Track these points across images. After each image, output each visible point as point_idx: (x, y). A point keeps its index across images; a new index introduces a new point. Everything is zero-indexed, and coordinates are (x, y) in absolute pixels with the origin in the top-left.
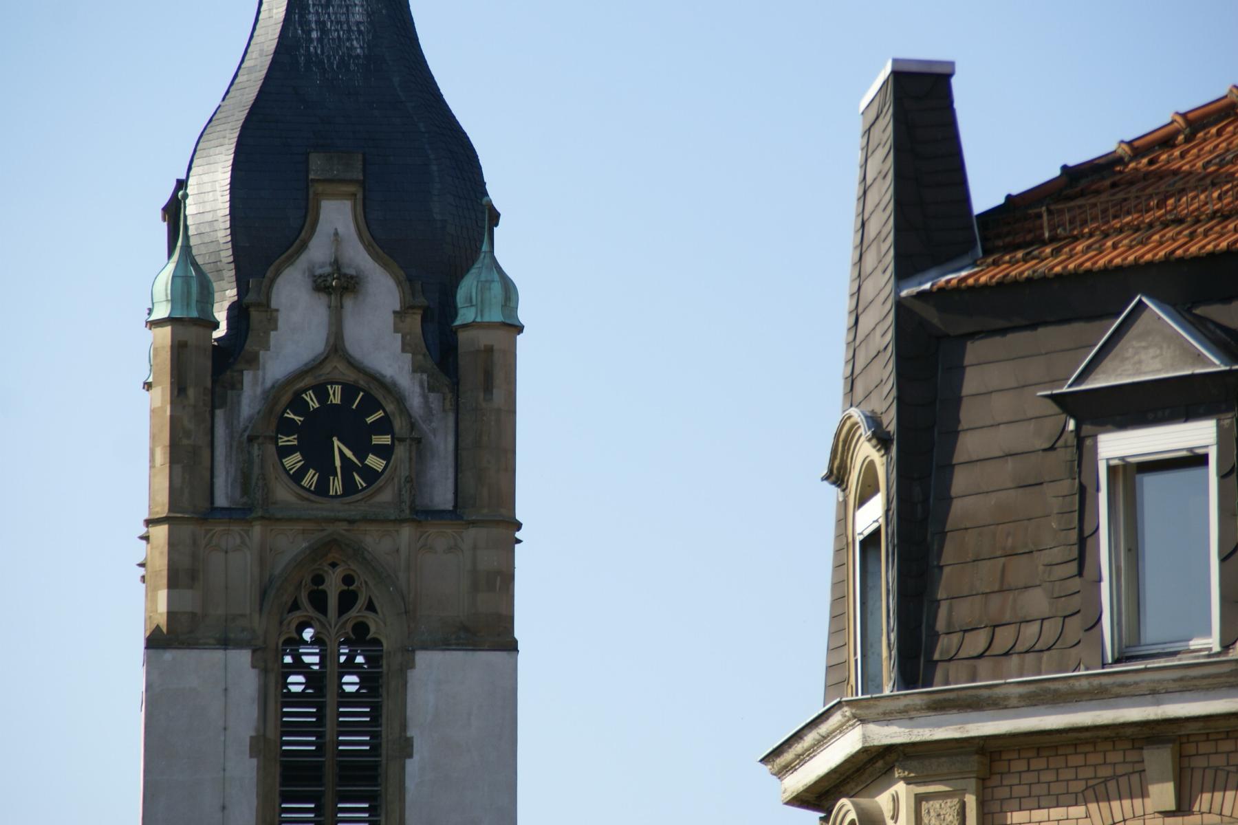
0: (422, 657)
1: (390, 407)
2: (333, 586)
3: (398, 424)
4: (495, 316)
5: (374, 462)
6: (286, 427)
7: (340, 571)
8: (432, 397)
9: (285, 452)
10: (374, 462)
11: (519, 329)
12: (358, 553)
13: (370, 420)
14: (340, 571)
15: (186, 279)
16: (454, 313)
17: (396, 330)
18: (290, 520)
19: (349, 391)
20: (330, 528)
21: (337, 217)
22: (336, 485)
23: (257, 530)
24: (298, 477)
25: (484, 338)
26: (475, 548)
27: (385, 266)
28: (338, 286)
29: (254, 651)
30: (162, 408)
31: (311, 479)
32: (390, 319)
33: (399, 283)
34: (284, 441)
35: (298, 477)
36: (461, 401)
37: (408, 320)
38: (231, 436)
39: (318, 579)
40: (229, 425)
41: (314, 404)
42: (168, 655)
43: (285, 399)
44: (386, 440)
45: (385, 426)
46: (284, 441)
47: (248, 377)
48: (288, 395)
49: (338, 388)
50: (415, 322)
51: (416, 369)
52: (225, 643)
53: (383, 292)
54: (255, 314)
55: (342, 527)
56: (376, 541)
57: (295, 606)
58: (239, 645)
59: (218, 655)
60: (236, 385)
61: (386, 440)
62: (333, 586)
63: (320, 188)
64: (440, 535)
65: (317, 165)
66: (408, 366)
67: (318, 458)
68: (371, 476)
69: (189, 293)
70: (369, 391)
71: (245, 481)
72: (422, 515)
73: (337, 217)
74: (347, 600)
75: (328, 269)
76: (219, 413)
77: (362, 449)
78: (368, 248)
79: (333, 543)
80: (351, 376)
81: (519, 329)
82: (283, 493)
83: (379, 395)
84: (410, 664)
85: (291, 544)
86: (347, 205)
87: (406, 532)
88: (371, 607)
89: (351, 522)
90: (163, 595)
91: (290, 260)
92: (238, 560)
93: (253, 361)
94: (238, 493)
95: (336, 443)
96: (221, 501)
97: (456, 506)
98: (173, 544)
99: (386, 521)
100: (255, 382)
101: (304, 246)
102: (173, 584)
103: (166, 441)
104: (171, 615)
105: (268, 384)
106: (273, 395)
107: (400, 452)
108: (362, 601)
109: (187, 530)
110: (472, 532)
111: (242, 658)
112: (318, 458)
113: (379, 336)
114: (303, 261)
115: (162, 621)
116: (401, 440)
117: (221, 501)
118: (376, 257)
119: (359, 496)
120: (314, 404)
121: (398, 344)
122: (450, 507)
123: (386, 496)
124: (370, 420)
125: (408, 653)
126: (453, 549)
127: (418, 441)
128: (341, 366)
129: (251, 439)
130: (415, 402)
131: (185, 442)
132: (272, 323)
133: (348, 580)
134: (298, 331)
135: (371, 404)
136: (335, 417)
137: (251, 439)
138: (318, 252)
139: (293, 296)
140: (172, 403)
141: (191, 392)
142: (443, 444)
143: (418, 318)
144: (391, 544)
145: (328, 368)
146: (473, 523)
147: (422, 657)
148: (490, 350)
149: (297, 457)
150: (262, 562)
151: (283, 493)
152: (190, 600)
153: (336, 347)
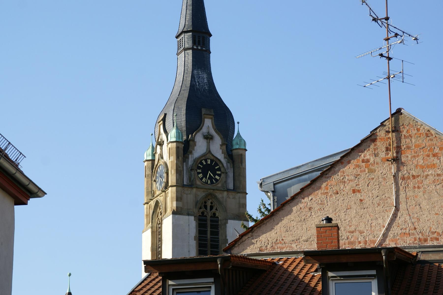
0: (230, 221)
1: (221, 165)
2: (209, 204)
3: (222, 169)
4: (243, 148)
5: (217, 177)
6: (199, 168)
7: (210, 201)
8: (228, 164)
9: (199, 173)
10: (217, 177)
11: (246, 150)
12: (215, 197)
13: (216, 168)
14: (210, 201)
15: (179, 133)
16: (232, 146)
17: (221, 149)
18: (201, 188)
19: (212, 161)
20: (209, 191)
21: (208, 123)
22: (209, 182)
23: (194, 190)
24: (201, 179)
25: (241, 152)
26: (239, 198)
27: (218, 134)
28: (208, 138)
29: (195, 217)
30: (174, 161)
31: (204, 180)
32: (219, 146)
33: (221, 138)
34: (198, 171)
35: (201, 179)
36: (235, 165)
37: (223, 147)
38: (187, 169)
39: (205, 202)
40: (187, 166)
41: (205, 163)
42: (177, 216)
43: (199, 162)
44: (219, 172)
45: (219, 169)
46: (198, 171)
47: (190, 156)
48: (198, 161)
49: (209, 160)
50: (224, 147)
51: (225, 158)
52: (188, 214)
53: (218, 140)
54: (191, 143)
55: (212, 191)
56: (219, 195)
57: (200, 208)
58: (191, 215)
59: (187, 217)
60: (188, 158)
61: (219, 172)
62: (209, 204)
63: (205, 116)
64: (231, 195)
65: (204, 111)
66: (223, 157)
67: (205, 176)
68: (217, 180)
69: (180, 136)
70: (216, 161)
71: (190, 179)
72: (228, 190)
73: (208, 123)
74: (212, 208)
75: (206, 134)
76: (184, 163)
77: (215, 174)
78: (215, 130)
79: (211, 194)
80: (212, 158)
81: (246, 150)
82: (198, 183)
83: (218, 162)
84: (227, 223)
85: (201, 194)
86: (210, 120)
87: (225, 193)
88: (216, 209)
89: (214, 190)
90: (175, 203)
91: (199, 131)
92: (191, 196)
93: (191, 153)
94: (188, 182)
95: (209, 172)
96: (185, 183)
97: (234, 189)
98: (177, 191)
99: (221, 190)
100: (192, 158)
101: (201, 128)
102: (177, 200)
103: (175, 168)
104: (177, 207)
105: (194, 158)
106: (195, 161)
107: (223, 175)
108: (214, 208)
109: (180, 189)
110: (239, 194)
111: (192, 218)
112: (205, 176)
113: (217, 150)
114: (201, 131)
115: (175, 209)
116: (223, 173)
117: (185, 183)
118: (216, 132)
119: (214, 185)
120: (205, 163)
121: (221, 152)
122: (232, 189)
123: (220, 185)
124: (216, 168)
125: (226, 220)
126: (234, 198)
127: (227, 173)
128: (211, 155)
129: (191, 170)
130: (225, 165)
131: (179, 169)
132: (195, 145)
133: (211, 203)
134: (200, 148)
135: (216, 164)
136: (208, 166)
137: (191, 170)
138: (204, 130)
139: (199, 139)
140: (176, 160)
141: (180, 158)
142: (231, 175)
143: (225, 147)
144: (222, 196)
145: (208, 156)
146: (239, 192)
147: (230, 221)
148: (241, 155)
149: (201, 175)
150: (196, 197)
151: (198, 183)
152: (181, 205)
153: (209, 151)
